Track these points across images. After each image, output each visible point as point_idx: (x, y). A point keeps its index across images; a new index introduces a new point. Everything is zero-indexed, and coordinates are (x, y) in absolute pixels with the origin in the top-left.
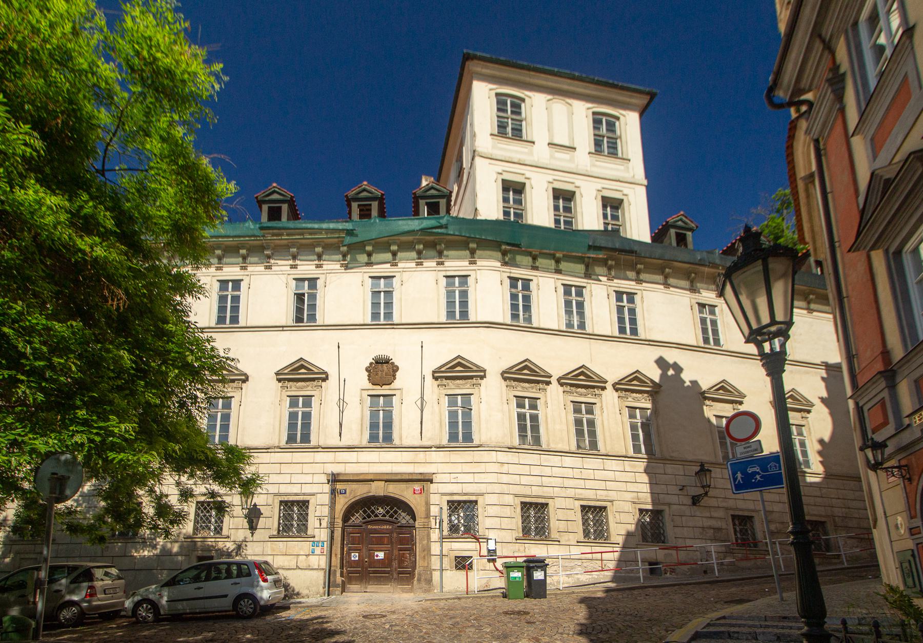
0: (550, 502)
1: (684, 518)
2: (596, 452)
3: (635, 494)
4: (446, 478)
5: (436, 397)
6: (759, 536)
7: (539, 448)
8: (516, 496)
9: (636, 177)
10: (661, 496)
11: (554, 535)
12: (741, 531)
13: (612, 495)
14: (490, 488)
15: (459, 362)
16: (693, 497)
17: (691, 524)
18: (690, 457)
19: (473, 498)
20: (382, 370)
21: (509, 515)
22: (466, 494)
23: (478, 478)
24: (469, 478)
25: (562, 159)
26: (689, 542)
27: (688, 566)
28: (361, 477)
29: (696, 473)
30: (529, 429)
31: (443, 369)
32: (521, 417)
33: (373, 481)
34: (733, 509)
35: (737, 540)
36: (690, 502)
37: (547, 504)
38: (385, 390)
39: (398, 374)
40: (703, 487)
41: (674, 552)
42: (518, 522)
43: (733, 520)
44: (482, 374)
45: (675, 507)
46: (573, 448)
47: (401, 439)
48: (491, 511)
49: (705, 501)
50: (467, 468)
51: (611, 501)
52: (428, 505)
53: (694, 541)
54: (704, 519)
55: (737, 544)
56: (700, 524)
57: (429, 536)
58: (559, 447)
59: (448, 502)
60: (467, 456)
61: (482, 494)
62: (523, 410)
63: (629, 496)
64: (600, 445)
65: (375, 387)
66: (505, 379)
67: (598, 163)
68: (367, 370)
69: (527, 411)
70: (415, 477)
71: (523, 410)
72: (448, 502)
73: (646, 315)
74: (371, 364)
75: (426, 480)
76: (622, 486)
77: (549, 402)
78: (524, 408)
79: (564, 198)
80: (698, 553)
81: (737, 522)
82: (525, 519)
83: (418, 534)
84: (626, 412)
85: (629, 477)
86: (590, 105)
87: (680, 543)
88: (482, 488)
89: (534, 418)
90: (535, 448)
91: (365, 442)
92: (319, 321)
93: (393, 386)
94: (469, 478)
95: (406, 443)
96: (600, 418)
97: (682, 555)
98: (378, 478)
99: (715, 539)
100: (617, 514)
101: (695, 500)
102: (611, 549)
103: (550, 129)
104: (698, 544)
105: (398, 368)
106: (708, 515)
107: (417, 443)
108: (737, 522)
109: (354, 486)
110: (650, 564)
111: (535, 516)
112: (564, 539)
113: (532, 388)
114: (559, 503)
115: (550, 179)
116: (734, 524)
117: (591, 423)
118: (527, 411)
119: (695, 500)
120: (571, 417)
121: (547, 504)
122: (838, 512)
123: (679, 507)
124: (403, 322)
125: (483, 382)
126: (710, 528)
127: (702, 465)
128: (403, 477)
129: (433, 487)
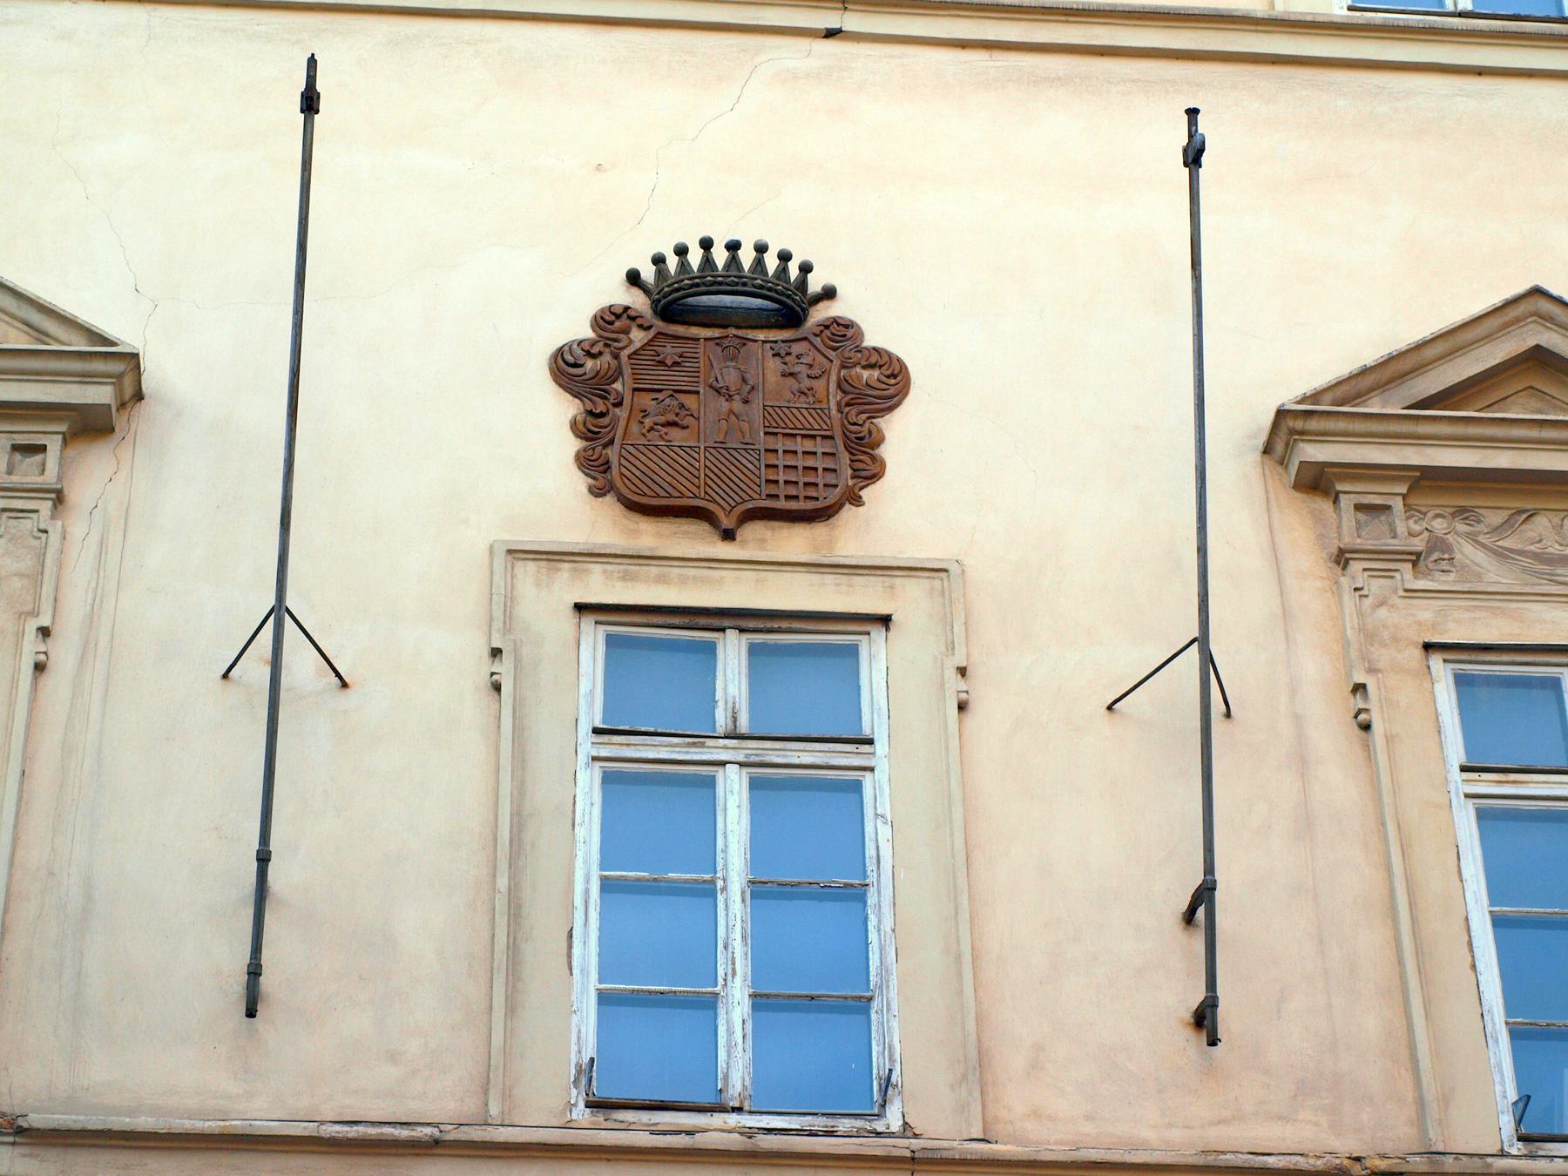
5: (1316, 670)
15: (1538, 358)
20: (726, 390)
31: (1374, 408)
38: (769, 572)
39: (901, 434)
47: (978, 1068)
65: (650, 535)
68: (566, 368)
74: (610, 321)
93: (853, 535)
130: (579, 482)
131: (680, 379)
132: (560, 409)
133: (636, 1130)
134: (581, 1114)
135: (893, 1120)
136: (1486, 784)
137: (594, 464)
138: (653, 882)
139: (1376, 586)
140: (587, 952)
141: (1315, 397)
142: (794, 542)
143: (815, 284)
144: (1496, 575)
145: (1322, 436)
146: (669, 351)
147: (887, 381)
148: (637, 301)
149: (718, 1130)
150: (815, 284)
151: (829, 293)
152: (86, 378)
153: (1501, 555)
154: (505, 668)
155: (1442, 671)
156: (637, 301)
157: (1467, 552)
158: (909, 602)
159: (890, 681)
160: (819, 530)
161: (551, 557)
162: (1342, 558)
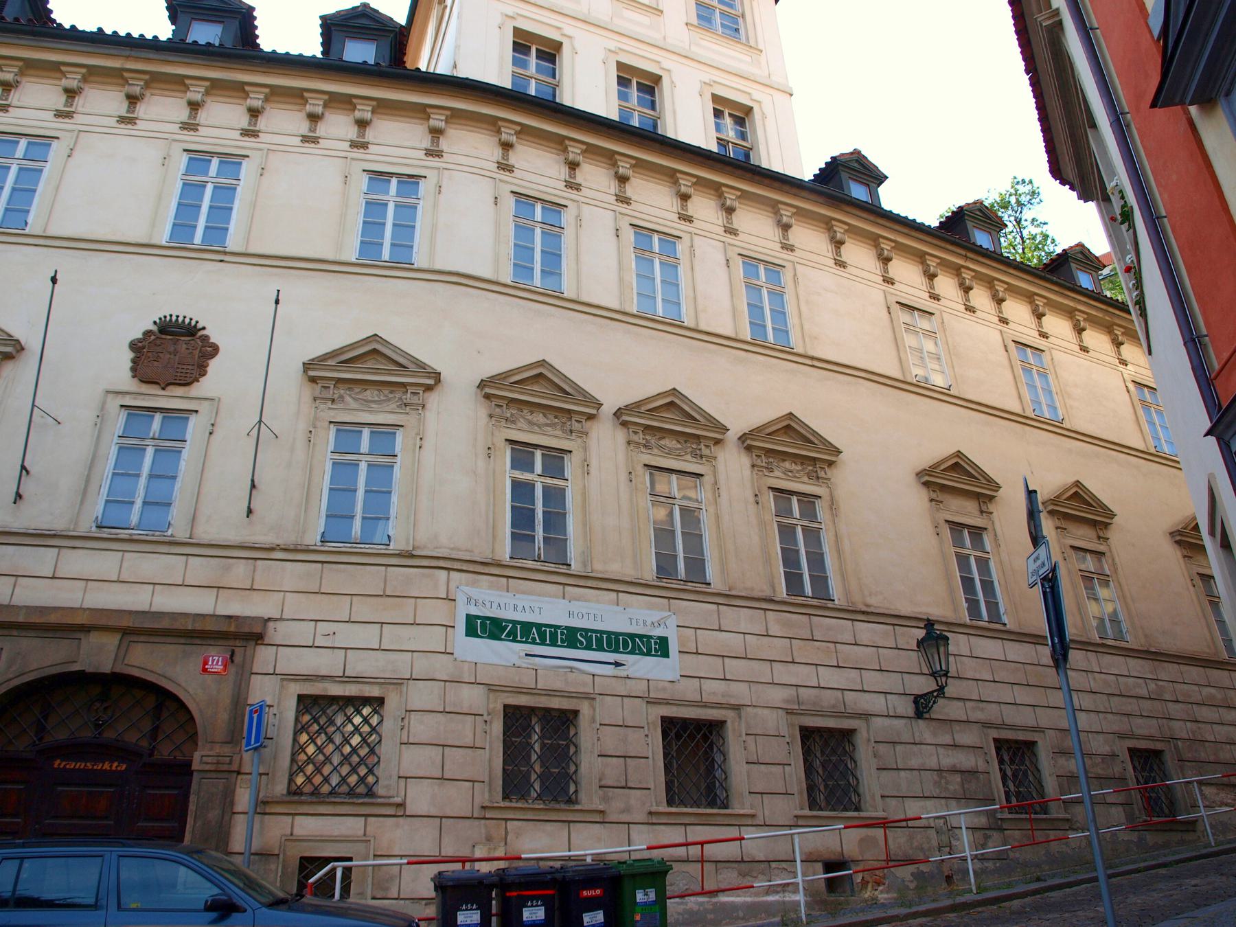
0: (585, 708)
1: (898, 748)
3: (792, 691)
4: (302, 633)
6: (1051, 786)
7: (563, 569)
8: (491, 688)
9: (773, 78)
10: (849, 696)
11: (589, 799)
12: (1015, 775)
13: (740, 693)
14: (422, 666)
15: (375, 351)
16: (917, 699)
17: (914, 763)
18: (905, 609)
19: (375, 692)
20: (172, 352)
21: (468, 741)
22: (356, 680)
23: (391, 637)
24: (367, 637)
26: (913, 808)
27: (912, 868)
28: (53, 619)
30: (537, 527)
31: (329, 363)
32: (521, 490)
33: (86, 629)
35: (1007, 794)
36: (910, 711)
37: (576, 713)
38: (173, 399)
39: (213, 365)
40: (934, 674)
42: (491, 759)
43: (998, 750)
44: (433, 381)
45: (878, 722)
46: (649, 571)
48: (421, 728)
49: (942, 708)
50: (363, 610)
51: (737, 708)
53: (921, 803)
54: (941, 750)
55: (1011, 809)
56: (933, 763)
57: (228, 798)
58: (616, 568)
59: (301, 698)
60: (369, 579)
61: (397, 683)
62: (527, 476)
63: (778, 696)
64: (712, 572)
65: (145, 388)
66: (487, 397)
68: (134, 346)
69: (536, 477)
70: (210, 626)
71: (527, 476)
72: (301, 698)
73: (804, 308)
74: (148, 333)
75: (242, 637)
76: (762, 671)
80: (932, 833)
81: (1006, 758)
82: (514, 750)
83: (200, 791)
85: (776, 648)
87: (894, 810)
88: (401, 665)
89: (555, 497)
90: (552, 567)
91: (86, 526)
92: (34, 223)
94: (367, 637)
95: (206, 532)
96: (711, 510)
97: (899, 840)
98: (103, 622)
99: (965, 798)
101: (922, 706)
104: (930, 811)
105: (216, 349)
106: (947, 739)
107: (232, 537)
108: (1006, 758)
109: (27, 644)
110: (829, 866)
112: (616, 806)
113: (552, 425)
114: (610, 710)
115: (612, 45)
116: (1001, 762)
118: (536, 477)
121: (576, 713)
122: (1181, 730)
123: (887, 721)
124: (251, 250)
125: (433, 399)
126: (954, 770)
128: (178, 625)
129: (263, 657)
130: (130, 374)
131: (159, 349)
132: (131, 355)
133: (105, 533)
134: (94, 529)
135: (169, 533)
136: (336, 456)
137: (134, 370)
138: (124, 473)
139: (322, 406)
140: (104, 490)
141: (313, 360)
142: (179, 391)
143: (200, 326)
144: (353, 405)
145: (314, 369)
146: (158, 342)
147: (216, 349)
148: (155, 328)
149: (123, 534)
150: (200, 326)
151: (204, 328)
152: (6, 345)
153: (355, 399)
154: (99, 420)
155: (333, 428)
156: (155, 328)
157: (348, 399)
158: (204, 407)
159: (195, 428)
160: (187, 388)
161: (117, 393)
162: (315, 399)
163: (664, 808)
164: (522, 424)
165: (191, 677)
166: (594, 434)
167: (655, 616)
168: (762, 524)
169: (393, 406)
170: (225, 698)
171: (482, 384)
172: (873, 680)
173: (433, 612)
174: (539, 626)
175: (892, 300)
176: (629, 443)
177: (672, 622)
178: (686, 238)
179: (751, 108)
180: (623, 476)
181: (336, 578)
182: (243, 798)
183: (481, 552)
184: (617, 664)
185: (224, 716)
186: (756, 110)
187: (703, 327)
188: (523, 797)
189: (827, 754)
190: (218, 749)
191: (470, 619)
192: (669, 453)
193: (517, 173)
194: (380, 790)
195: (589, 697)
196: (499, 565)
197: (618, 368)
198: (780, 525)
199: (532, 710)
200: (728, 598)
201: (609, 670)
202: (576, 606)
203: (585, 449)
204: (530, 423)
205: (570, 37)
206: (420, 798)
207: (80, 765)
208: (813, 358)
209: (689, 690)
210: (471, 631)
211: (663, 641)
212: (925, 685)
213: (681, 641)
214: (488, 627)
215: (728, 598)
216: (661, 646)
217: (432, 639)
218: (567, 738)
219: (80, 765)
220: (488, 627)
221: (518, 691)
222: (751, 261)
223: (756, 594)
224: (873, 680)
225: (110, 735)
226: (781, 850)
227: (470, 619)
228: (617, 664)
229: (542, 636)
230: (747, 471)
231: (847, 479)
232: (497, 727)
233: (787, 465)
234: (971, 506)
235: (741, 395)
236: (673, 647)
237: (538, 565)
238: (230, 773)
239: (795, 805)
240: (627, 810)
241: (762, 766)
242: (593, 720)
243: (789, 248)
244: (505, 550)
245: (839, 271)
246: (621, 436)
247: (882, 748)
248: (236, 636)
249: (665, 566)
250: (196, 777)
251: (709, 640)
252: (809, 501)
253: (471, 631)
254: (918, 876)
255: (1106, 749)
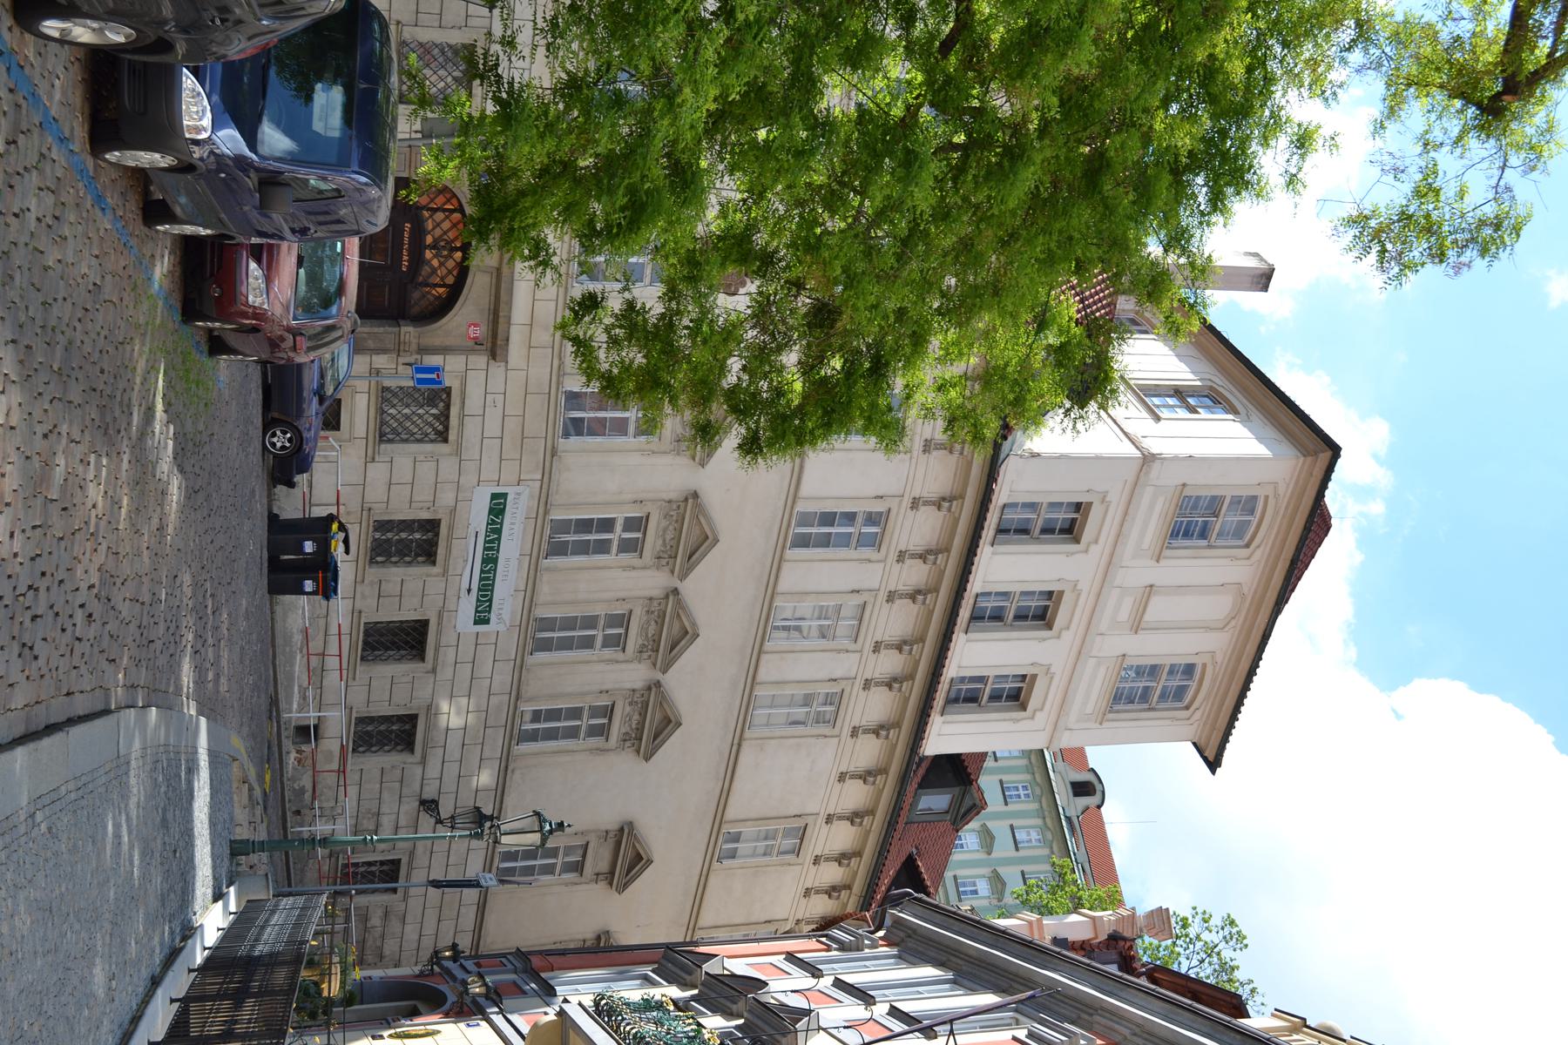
1: (397, 785)
2: (529, 648)
4: (496, 383)
11: (374, 573)
12: (372, 873)
16: (435, 802)
17: (385, 795)
19: (452, 436)
24: (493, 428)
25: (1119, 607)
26: (352, 791)
27: (309, 787)
29: (478, 809)
32: (607, 525)
34: (410, 863)
35: (356, 865)
36: (426, 796)
37: (434, 563)
40: (453, 817)
41: (335, 766)
43: (392, 862)
45: (419, 771)
46: (542, 612)
48: (426, 470)
49: (427, 821)
50: (512, 424)
51: (434, 671)
52: (444, 350)
53: (355, 798)
55: (346, 866)
57: (383, 351)
60: (536, 425)
61: (458, 452)
62: (619, 527)
64: (542, 656)
67: (1102, 670)
70: (501, 327)
73: (792, 741)
75: (494, 346)
77: (633, 574)
78: (625, 530)
79: (1039, 613)
80: (332, 804)
81: (385, 868)
84: (604, 701)
86: (1219, 658)
87: (352, 777)
88: (471, 452)
89: (603, 547)
90: (545, 546)
100: (409, 679)
101: (430, 805)
102: (345, 666)
103: (1181, 589)
104: (350, 804)
108: (385, 868)
110: (316, 727)
111: (414, 541)
116: (382, 863)
117: (588, 643)
119: (430, 805)
120: (600, 610)
123: (419, 778)
127: (491, 818)
128: (502, 305)
129: (480, 361)
163: (363, 621)
164: (664, 523)
165: (465, 317)
166: (656, 573)
167: (506, 616)
168: (584, 694)
169: (680, 430)
170: (448, 342)
171: (695, 495)
172: (452, 770)
173: (509, 473)
174: (499, 539)
175: (810, 820)
176: (651, 599)
177: (501, 628)
178: (852, 647)
179: (1025, 709)
180: (622, 595)
181: (536, 404)
182: (381, 361)
183: (556, 499)
184: (469, 591)
185: (437, 342)
186: (1022, 714)
187: (764, 657)
188: (376, 530)
189: (396, 733)
190: (414, 341)
191: (504, 496)
192: (643, 629)
193: (911, 514)
194: (383, 446)
195: (445, 573)
196: (546, 513)
197: (719, 593)
198: (581, 709)
199: (437, 535)
200: (520, 667)
201: (465, 585)
202: (514, 563)
203: (644, 568)
204: (665, 530)
205: (1086, 551)
206: (378, 472)
207: (406, 240)
208: (739, 745)
209: (449, 638)
210: (494, 496)
211: (487, 622)
212: (446, 810)
213: (486, 634)
214: (498, 507)
215: (520, 667)
216: (481, 620)
217: (489, 471)
218: (417, 555)
219: (406, 240)
220: (498, 507)
221: (451, 528)
222: (835, 700)
223: (523, 688)
224: (452, 770)
225: (428, 254)
226: (329, 698)
227: (504, 496)
228: (469, 591)
229: (492, 541)
230: (629, 686)
231: (625, 764)
232: (425, 515)
233: (636, 717)
234: (604, 866)
235: (700, 684)
236: (481, 628)
237: (546, 538)
238: (398, 350)
239: (361, 710)
240: (364, 597)
241: (389, 686)
242: (428, 575)
243: (855, 732)
244: (557, 515)
245: (835, 775)
246: (657, 593)
247: (399, 772)
248: (494, 343)
249: (548, 624)
250: (396, 329)
251: (486, 654)
252: (601, 731)
253: (494, 496)
254: (302, 790)
255: (387, 952)
